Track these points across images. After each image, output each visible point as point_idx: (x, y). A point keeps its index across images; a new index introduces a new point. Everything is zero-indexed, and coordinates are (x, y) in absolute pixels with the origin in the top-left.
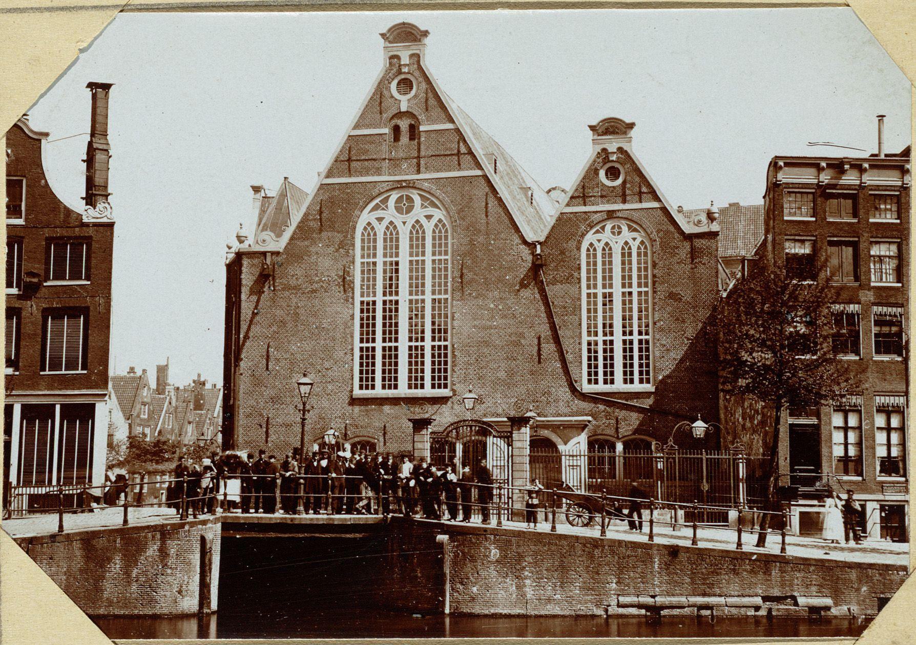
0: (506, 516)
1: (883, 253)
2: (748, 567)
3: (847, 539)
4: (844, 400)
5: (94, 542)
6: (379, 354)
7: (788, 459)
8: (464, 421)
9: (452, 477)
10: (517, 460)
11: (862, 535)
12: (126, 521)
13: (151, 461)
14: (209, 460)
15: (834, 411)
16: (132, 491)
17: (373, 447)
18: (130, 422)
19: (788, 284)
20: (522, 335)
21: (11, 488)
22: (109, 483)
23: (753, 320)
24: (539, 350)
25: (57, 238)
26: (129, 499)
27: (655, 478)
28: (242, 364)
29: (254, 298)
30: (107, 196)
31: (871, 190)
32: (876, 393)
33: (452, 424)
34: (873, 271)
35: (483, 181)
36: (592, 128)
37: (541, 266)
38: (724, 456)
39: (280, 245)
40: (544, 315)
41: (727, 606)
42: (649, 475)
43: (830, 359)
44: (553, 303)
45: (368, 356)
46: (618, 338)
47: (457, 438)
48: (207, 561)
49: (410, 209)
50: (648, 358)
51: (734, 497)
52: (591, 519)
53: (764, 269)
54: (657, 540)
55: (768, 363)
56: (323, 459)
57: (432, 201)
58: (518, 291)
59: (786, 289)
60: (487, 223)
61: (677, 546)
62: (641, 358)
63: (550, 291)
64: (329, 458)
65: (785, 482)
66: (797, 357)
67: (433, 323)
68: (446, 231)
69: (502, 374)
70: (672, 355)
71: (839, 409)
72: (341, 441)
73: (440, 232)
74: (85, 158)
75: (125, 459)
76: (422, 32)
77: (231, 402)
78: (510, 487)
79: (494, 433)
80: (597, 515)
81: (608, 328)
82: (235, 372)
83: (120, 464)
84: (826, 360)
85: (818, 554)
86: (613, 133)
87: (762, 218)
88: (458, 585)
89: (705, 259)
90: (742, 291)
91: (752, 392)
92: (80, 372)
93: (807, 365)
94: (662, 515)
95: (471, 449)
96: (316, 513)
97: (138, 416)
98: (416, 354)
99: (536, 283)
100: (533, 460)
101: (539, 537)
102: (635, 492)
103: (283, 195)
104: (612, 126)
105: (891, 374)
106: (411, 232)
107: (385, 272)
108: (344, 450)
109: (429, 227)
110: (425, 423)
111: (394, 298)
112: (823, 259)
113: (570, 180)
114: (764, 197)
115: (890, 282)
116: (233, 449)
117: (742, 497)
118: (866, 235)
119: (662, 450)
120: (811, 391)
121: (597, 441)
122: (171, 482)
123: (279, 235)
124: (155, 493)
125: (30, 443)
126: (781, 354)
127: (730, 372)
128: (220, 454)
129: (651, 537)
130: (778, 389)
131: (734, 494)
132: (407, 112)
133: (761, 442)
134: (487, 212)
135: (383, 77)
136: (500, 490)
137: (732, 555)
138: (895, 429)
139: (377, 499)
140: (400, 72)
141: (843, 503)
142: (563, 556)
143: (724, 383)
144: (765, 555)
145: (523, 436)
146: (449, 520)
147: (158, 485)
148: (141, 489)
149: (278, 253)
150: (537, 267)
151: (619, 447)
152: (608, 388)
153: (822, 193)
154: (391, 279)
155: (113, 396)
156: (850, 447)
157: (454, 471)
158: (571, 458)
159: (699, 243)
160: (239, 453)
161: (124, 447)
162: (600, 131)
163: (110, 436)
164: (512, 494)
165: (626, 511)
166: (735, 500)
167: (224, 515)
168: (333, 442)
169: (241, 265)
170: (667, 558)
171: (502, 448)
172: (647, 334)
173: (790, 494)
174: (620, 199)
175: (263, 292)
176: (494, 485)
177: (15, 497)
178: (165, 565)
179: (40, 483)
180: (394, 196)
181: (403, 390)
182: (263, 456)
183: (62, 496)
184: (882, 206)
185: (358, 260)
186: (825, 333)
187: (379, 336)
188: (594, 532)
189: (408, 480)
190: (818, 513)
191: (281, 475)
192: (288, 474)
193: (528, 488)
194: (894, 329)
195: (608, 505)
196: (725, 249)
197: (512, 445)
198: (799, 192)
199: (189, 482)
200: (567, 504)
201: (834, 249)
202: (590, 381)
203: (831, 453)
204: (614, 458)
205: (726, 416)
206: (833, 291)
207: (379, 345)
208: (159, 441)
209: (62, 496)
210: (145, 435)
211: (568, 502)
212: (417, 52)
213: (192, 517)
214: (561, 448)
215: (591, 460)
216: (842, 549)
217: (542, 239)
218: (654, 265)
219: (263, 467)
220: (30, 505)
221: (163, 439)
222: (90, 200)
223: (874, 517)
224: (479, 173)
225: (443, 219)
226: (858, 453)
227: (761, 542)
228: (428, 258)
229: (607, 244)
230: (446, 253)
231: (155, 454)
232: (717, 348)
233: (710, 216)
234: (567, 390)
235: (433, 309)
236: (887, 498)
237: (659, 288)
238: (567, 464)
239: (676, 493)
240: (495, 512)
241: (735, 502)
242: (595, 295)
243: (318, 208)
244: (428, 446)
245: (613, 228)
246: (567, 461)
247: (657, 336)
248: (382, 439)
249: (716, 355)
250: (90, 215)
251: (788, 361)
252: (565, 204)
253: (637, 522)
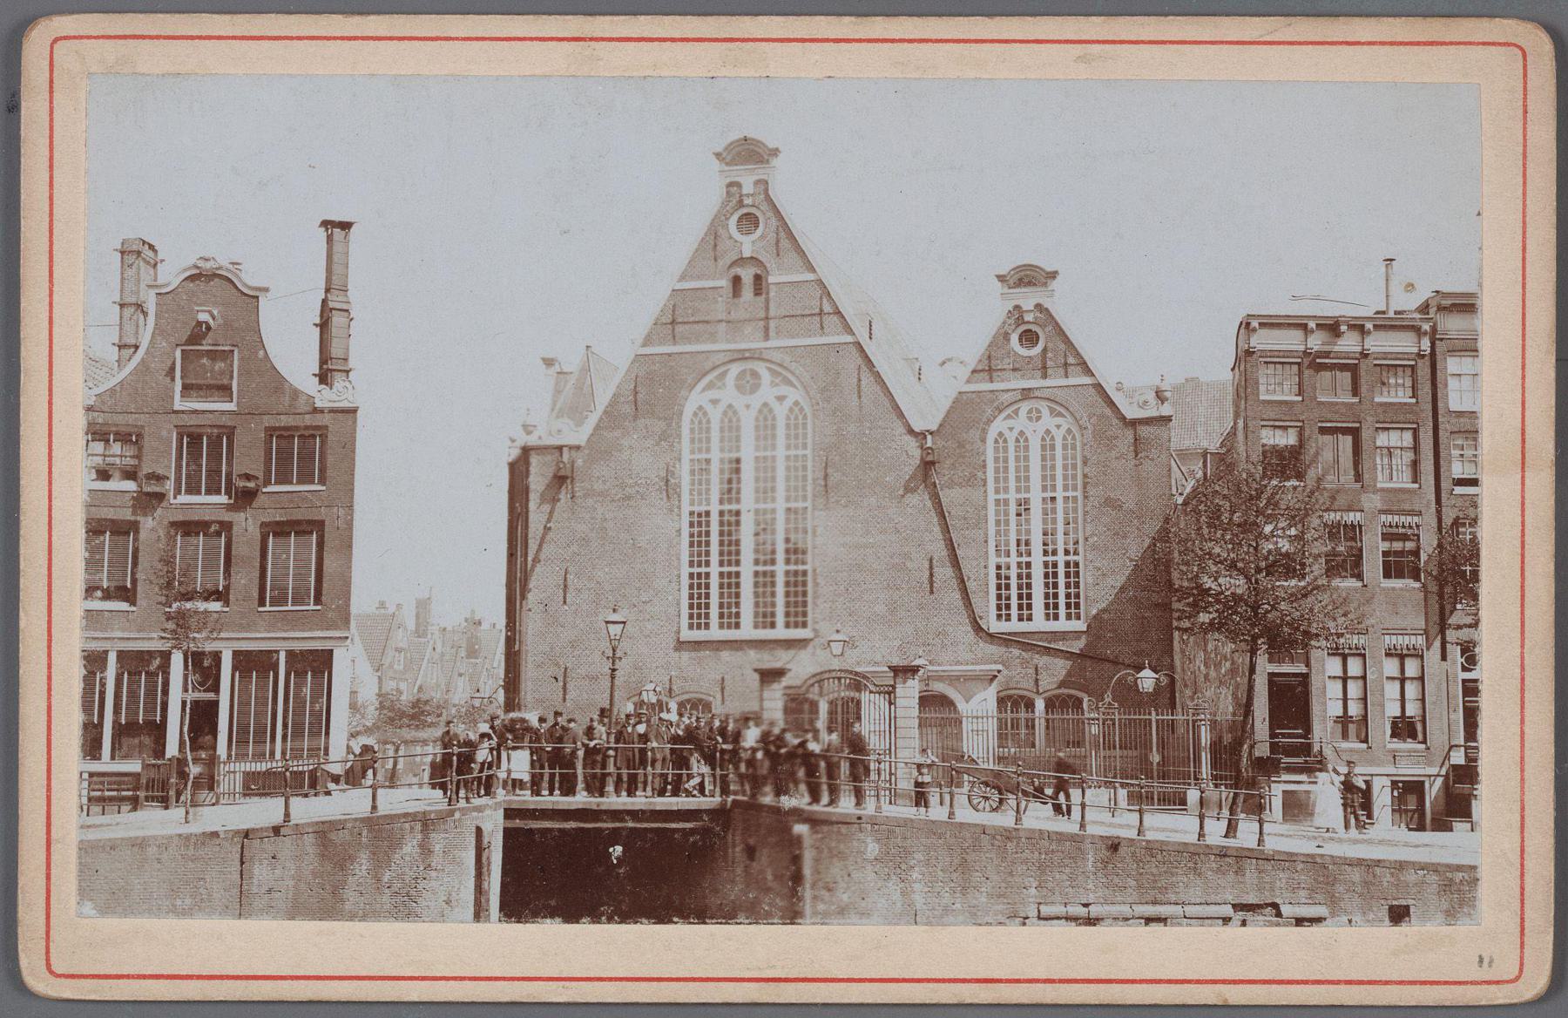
0: (888, 798)
1: (1392, 444)
2: (1214, 865)
3: (1347, 826)
4: (1342, 640)
5: (333, 836)
6: (714, 581)
7: (1267, 719)
8: (830, 671)
9: (814, 747)
10: (900, 723)
11: (1367, 821)
12: (374, 808)
13: (409, 726)
14: (487, 726)
15: (1328, 654)
16: (383, 767)
17: (707, 706)
18: (379, 674)
19: (1266, 486)
20: (907, 556)
21: (220, 763)
22: (351, 757)
23: (1219, 533)
24: (931, 575)
25: (280, 428)
26: (380, 777)
27: (1088, 747)
28: (530, 596)
29: (547, 508)
30: (347, 372)
31: (1376, 359)
32: (1385, 632)
33: (814, 676)
34: (1379, 467)
35: (853, 350)
36: (1001, 278)
37: (933, 463)
38: (1180, 717)
39: (580, 436)
40: (937, 529)
41: (1185, 917)
42: (1078, 744)
43: (1323, 585)
44: (949, 513)
45: (699, 584)
46: (1037, 560)
47: (821, 694)
48: (484, 860)
49: (755, 388)
50: (1077, 585)
51: (1195, 772)
52: (1001, 801)
53: (1231, 467)
54: (1091, 830)
55: (1239, 591)
56: (640, 722)
57: (785, 377)
58: (903, 496)
59: (1262, 493)
60: (861, 407)
61: (1118, 837)
62: (1068, 586)
63: (946, 496)
64: (648, 721)
65: (1263, 750)
66: (1278, 583)
67: (787, 540)
68: (805, 417)
69: (880, 609)
70: (1110, 581)
71: (1335, 652)
72: (665, 699)
73: (796, 418)
74: (318, 321)
75: (374, 724)
76: (770, 150)
77: (517, 647)
78: (893, 759)
79: (872, 688)
80: (1010, 796)
81: (1024, 545)
82: (521, 607)
83: (368, 731)
84: (1317, 588)
85: (1308, 847)
86: (1030, 284)
87: (1230, 398)
88: (824, 892)
89: (1154, 453)
90: (1205, 496)
91: (1218, 629)
92: (312, 607)
93: (1292, 595)
94: (1097, 796)
95: (839, 709)
96: (630, 793)
97: (391, 666)
98: (764, 581)
99: (926, 486)
100: (922, 724)
101: (932, 828)
102: (1062, 766)
103: (586, 369)
104: (1027, 276)
105: (1405, 606)
106: (757, 419)
107: (722, 471)
108: (668, 711)
109: (781, 411)
110: (777, 674)
111: (734, 507)
112: (1312, 451)
113: (973, 350)
114: (1233, 369)
115: (1403, 482)
116: (520, 710)
117: (1205, 770)
118: (1369, 419)
119: (1097, 708)
120: (1297, 629)
121: (1009, 697)
122: (435, 754)
123: (579, 423)
124: (415, 771)
125: (245, 703)
126: (1257, 582)
127: (1188, 604)
128: (502, 717)
129: (1082, 826)
130: (1253, 625)
131: (1195, 767)
132: (752, 258)
133: (1230, 698)
134: (859, 392)
135: (719, 211)
136: (880, 763)
137: (1192, 849)
138: (1412, 679)
139: (714, 776)
140: (741, 204)
141: (1342, 778)
142: (964, 850)
143: (1179, 619)
144: (1237, 849)
145: (909, 692)
146: (810, 804)
147: (418, 759)
148: (395, 764)
149: (578, 448)
150: (927, 465)
151: (1040, 705)
152: (1025, 626)
153: (1314, 363)
154: (730, 481)
155: (357, 639)
156: (1350, 703)
157: (816, 739)
158: (975, 720)
159: (1144, 431)
160: (527, 716)
161: (372, 708)
162: (1011, 282)
163: (353, 693)
164: (896, 768)
165: (1049, 791)
166: (1195, 776)
167: (507, 798)
168: (654, 700)
169: (527, 463)
170: (1105, 853)
171: (882, 707)
172: (1076, 553)
173: (1267, 767)
174: (1039, 373)
175: (559, 500)
176: (872, 757)
177: (225, 776)
178: (428, 867)
179: (259, 756)
180: (735, 369)
181: (747, 631)
182: (559, 719)
183: (288, 774)
184: (1392, 381)
185: (686, 456)
186: (1315, 551)
187: (714, 558)
188: (1005, 819)
189: (754, 750)
190: (1308, 792)
191: (583, 744)
192: (592, 744)
193: (916, 761)
194: (1410, 545)
195: (1024, 782)
196: (1179, 438)
197: (895, 704)
198: (1280, 363)
199: (459, 755)
200: (969, 782)
201: (1328, 438)
202: (999, 617)
203: (1325, 711)
204: (1033, 720)
205: (1183, 663)
206: (1326, 494)
207: (714, 570)
208: (418, 700)
209: (288, 774)
210: (400, 692)
211: (971, 779)
212: (765, 177)
213: (464, 801)
214: (961, 706)
215: (1002, 724)
216: (1340, 841)
217: (934, 427)
218: (1085, 463)
219: (559, 734)
220: (246, 786)
221: (424, 697)
222: (324, 377)
223: (1383, 798)
224: (849, 339)
225: (800, 401)
226: (1363, 713)
227: (1231, 829)
228: (781, 452)
229: (1022, 433)
230: (805, 447)
231: (413, 717)
232: (1169, 573)
233: (1160, 396)
234: (969, 628)
235: (788, 521)
236: (1401, 772)
237: (1092, 491)
238: (970, 728)
239: (1115, 767)
240: (872, 793)
241: (1196, 779)
242: (1006, 502)
243: (632, 387)
244: (780, 704)
245: (1030, 411)
246: (970, 725)
247: (1090, 557)
248: (719, 696)
249: (1170, 583)
250: (325, 398)
251: (1266, 590)
252: (965, 380)
253: (1064, 807)
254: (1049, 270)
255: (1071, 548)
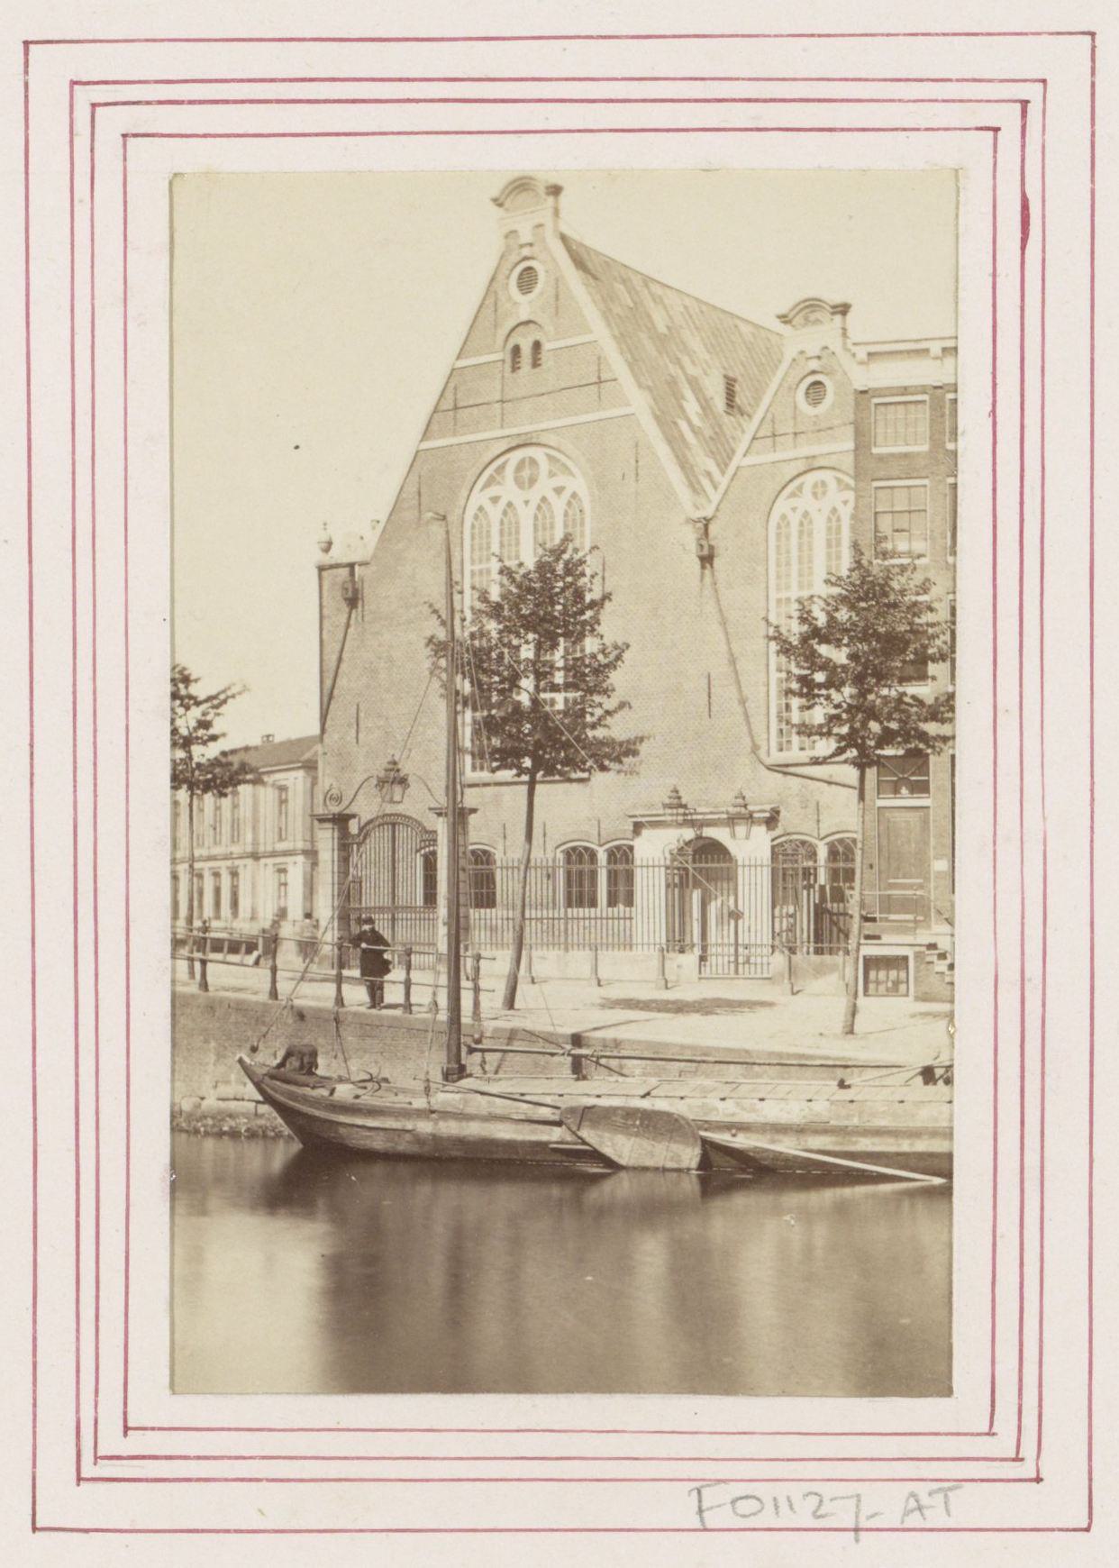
49: (532, 481)
57: (564, 465)
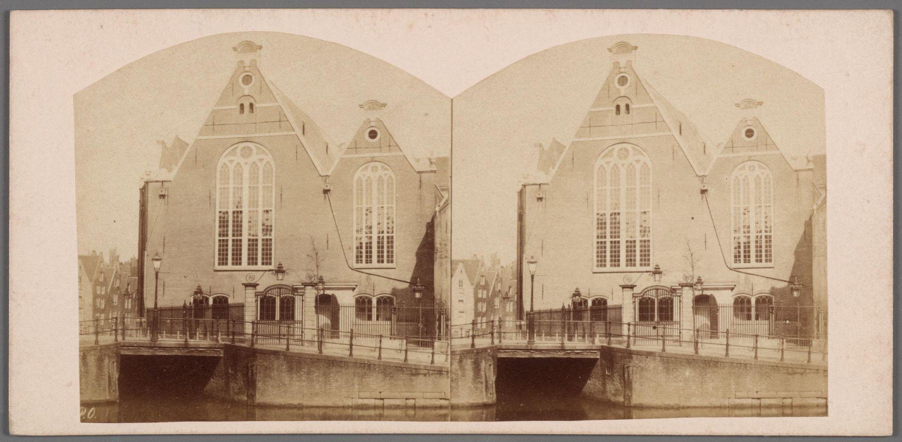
6: (230, 243)
45: (223, 244)
207: (230, 238)
254: (382, 102)
255: (390, 230)
